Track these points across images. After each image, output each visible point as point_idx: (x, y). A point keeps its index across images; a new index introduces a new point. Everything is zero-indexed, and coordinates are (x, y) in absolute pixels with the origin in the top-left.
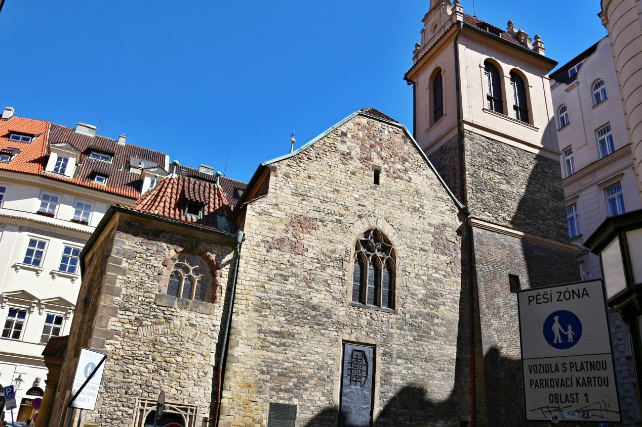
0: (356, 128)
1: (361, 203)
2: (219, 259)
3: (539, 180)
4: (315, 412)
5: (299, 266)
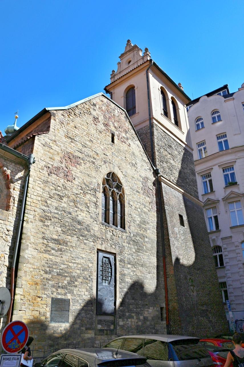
0: (101, 103)
1: (105, 153)
2: (13, 175)
3: (185, 162)
4: (82, 305)
5: (70, 190)
